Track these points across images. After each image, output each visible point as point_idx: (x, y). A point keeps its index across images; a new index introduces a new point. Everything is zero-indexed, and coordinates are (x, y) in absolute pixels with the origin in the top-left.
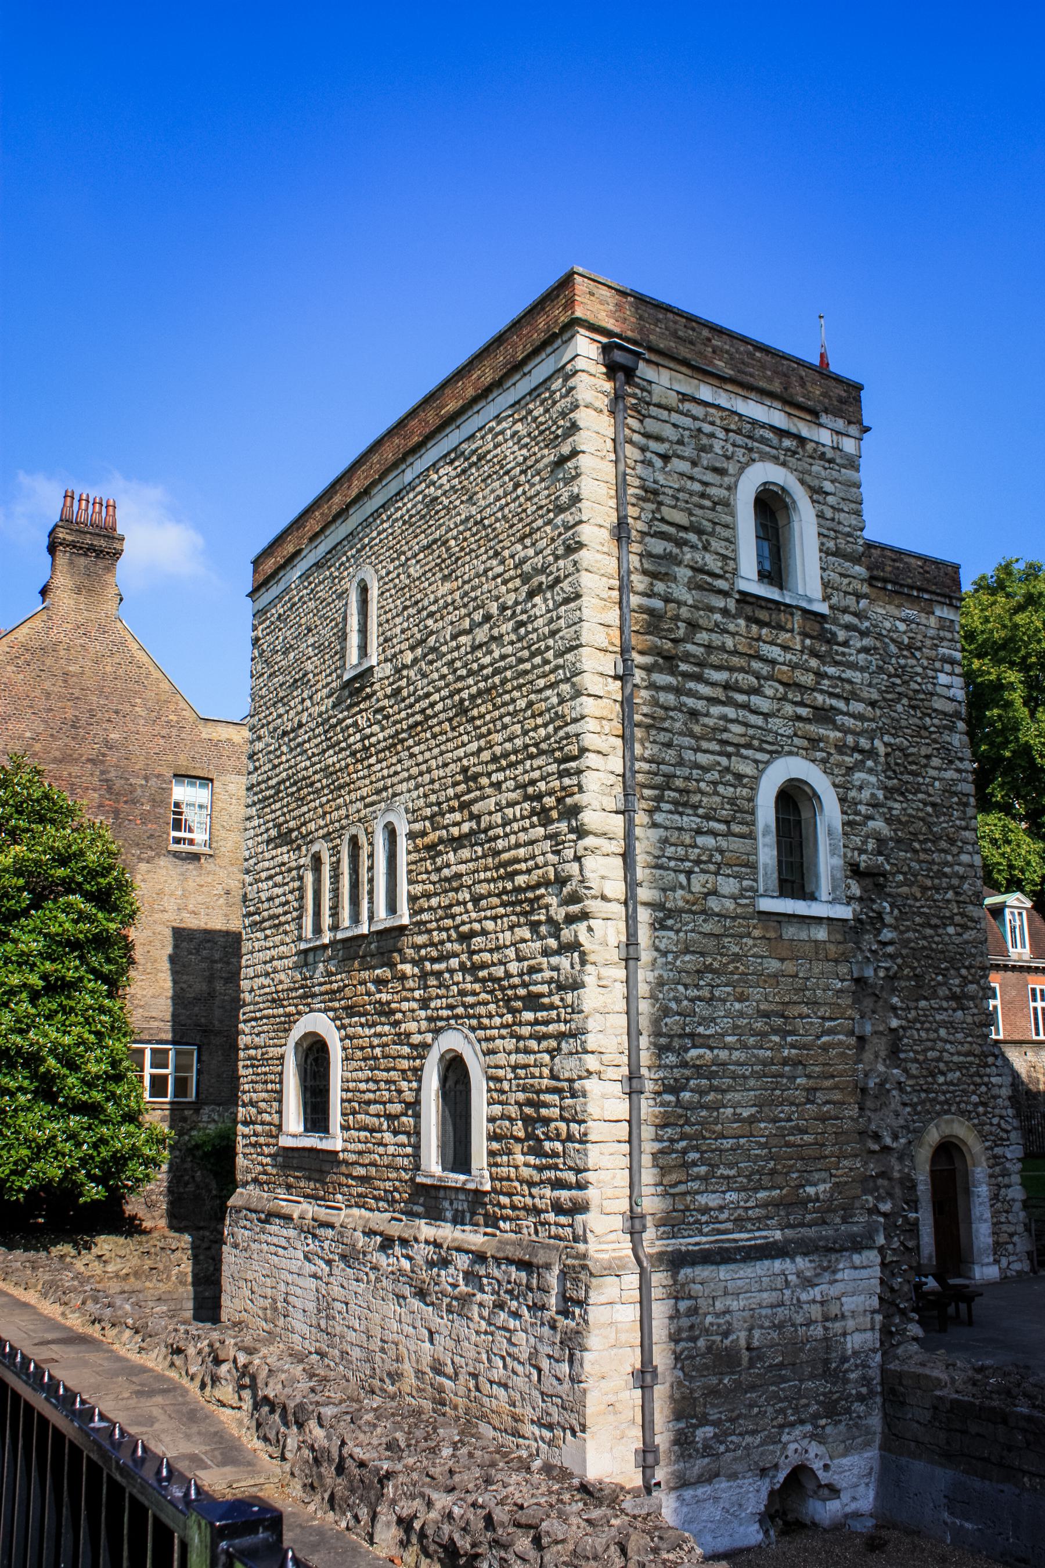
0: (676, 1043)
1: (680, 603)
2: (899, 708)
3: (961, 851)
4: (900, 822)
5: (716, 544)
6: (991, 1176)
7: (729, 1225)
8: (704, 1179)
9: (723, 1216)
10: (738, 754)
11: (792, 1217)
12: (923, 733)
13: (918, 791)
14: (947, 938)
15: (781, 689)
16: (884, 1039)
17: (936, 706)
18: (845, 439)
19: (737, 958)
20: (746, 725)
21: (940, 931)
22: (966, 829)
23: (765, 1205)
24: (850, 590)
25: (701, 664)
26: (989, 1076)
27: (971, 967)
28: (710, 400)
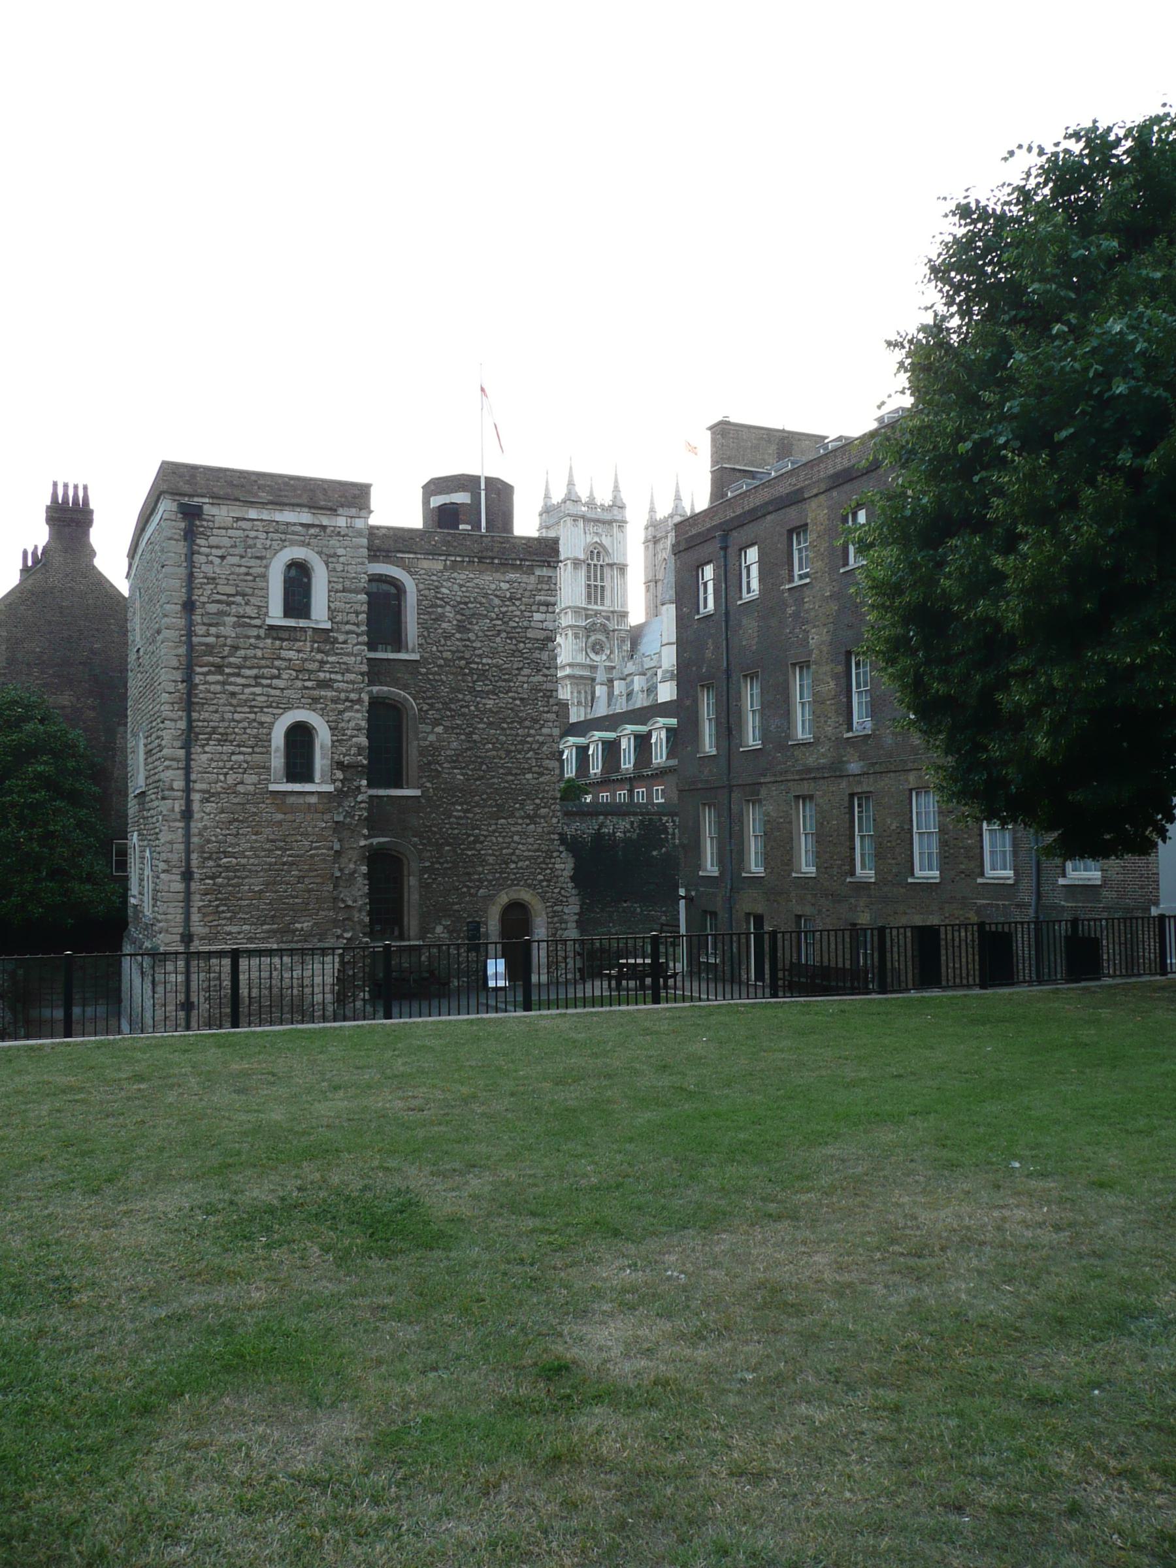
0: (214, 856)
1: (226, 637)
2: (498, 640)
3: (543, 726)
4: (493, 712)
5: (253, 600)
6: (548, 923)
7: (245, 941)
8: (230, 919)
9: (239, 937)
10: (262, 712)
11: (284, 939)
12: (516, 654)
13: (509, 691)
14: (524, 781)
15: (294, 673)
16: (356, 852)
17: (529, 635)
18: (357, 520)
19: (255, 814)
20: (268, 696)
21: (519, 777)
22: (548, 712)
23: (268, 931)
24: (352, 610)
25: (239, 668)
26: (554, 864)
27: (543, 798)
28: (255, 517)
